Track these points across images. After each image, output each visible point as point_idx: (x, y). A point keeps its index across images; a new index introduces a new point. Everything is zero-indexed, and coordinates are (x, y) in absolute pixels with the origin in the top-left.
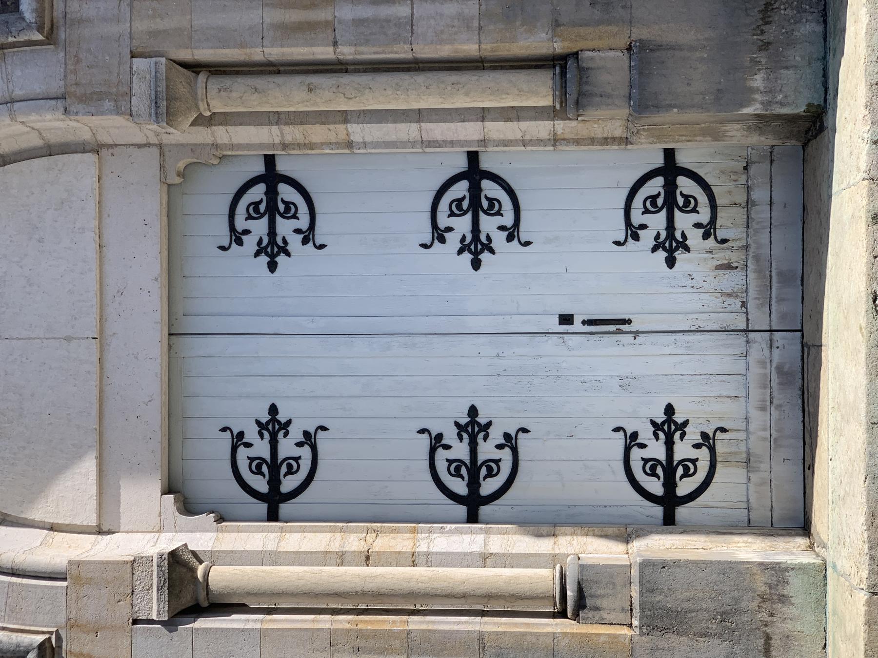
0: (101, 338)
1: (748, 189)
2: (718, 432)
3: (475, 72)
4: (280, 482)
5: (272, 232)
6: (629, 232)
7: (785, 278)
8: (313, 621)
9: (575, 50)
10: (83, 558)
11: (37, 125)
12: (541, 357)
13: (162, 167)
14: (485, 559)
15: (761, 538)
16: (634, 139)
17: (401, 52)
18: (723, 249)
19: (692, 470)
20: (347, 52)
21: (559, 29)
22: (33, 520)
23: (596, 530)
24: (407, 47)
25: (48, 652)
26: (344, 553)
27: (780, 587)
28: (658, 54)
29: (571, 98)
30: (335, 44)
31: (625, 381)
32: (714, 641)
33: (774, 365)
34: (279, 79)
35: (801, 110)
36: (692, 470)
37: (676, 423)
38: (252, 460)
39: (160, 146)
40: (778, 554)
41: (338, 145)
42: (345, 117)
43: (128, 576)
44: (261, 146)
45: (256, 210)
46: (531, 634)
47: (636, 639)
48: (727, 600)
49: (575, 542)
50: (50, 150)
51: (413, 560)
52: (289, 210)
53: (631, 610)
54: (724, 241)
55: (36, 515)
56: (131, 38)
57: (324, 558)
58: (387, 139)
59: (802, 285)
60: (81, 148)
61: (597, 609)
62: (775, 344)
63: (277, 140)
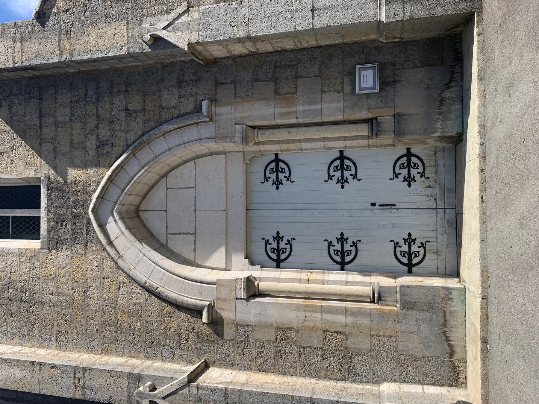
0: (226, 211)
1: (436, 161)
2: (427, 242)
3: (342, 125)
4: (280, 256)
5: (277, 177)
6: (395, 176)
7: (449, 190)
8: (291, 301)
9: (375, 117)
10: (221, 278)
11: (208, 146)
12: (364, 217)
13: (244, 158)
14: (347, 283)
15: (442, 278)
16: (396, 145)
17: (318, 120)
18: (428, 181)
19: (418, 255)
20: (301, 121)
21: (370, 110)
22: (206, 266)
23: (385, 274)
24: (320, 118)
25: (211, 307)
26: (301, 279)
27: (449, 295)
28: (404, 117)
29: (374, 132)
30: (297, 118)
31: (394, 225)
32: (426, 313)
33: (446, 220)
34: (280, 130)
35: (454, 134)
36: (418, 255)
37: (412, 239)
38: (271, 248)
39: (244, 152)
40: (448, 284)
41: (298, 150)
42: (300, 141)
43: (235, 284)
44: (274, 151)
45: (273, 171)
46: (363, 308)
47: (399, 311)
48: (430, 299)
49: (377, 278)
50: (212, 154)
51: (323, 282)
52: (283, 171)
53: (397, 301)
54: (428, 178)
55: (207, 264)
56: (235, 119)
57: (294, 280)
58: (314, 147)
59: (456, 193)
60: (220, 153)
61: (385, 301)
62: (446, 213)
63: (279, 149)
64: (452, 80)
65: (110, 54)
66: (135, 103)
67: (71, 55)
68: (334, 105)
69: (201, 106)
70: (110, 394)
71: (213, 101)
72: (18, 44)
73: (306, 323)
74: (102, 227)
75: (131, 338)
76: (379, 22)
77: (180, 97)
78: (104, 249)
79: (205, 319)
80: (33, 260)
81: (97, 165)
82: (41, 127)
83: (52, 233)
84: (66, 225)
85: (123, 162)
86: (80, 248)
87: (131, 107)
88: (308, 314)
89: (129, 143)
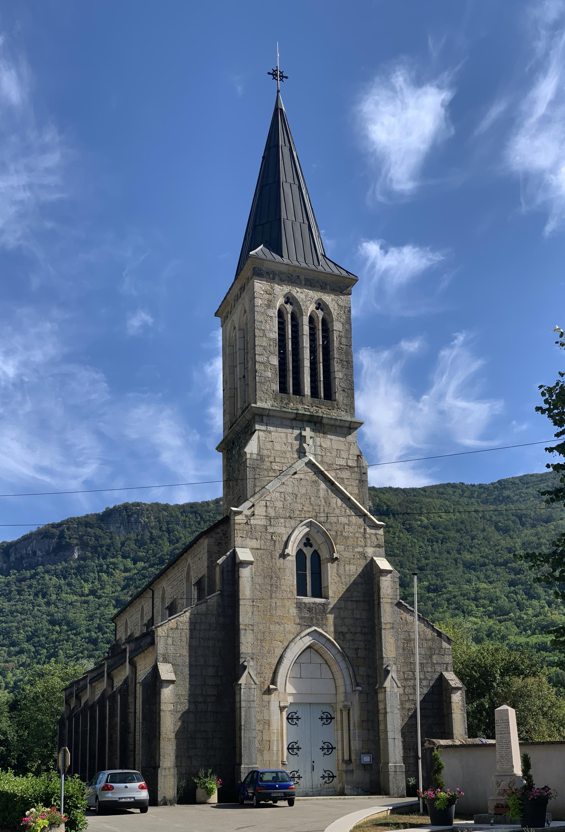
20: (351, 731)
64: (365, 791)
65: (383, 648)
66: (361, 653)
67: (384, 629)
68: (357, 746)
69: (359, 686)
70: (244, 644)
71: (361, 692)
72: (389, 601)
73: (272, 733)
74: (308, 634)
75: (259, 648)
76: (388, 763)
77: (363, 676)
78: (298, 635)
79: (272, 687)
80: (291, 593)
81: (335, 632)
82: (352, 601)
83: (303, 605)
84: (307, 613)
85: (337, 647)
86: (298, 621)
87: (359, 651)
88: (276, 734)
89: (344, 649)
